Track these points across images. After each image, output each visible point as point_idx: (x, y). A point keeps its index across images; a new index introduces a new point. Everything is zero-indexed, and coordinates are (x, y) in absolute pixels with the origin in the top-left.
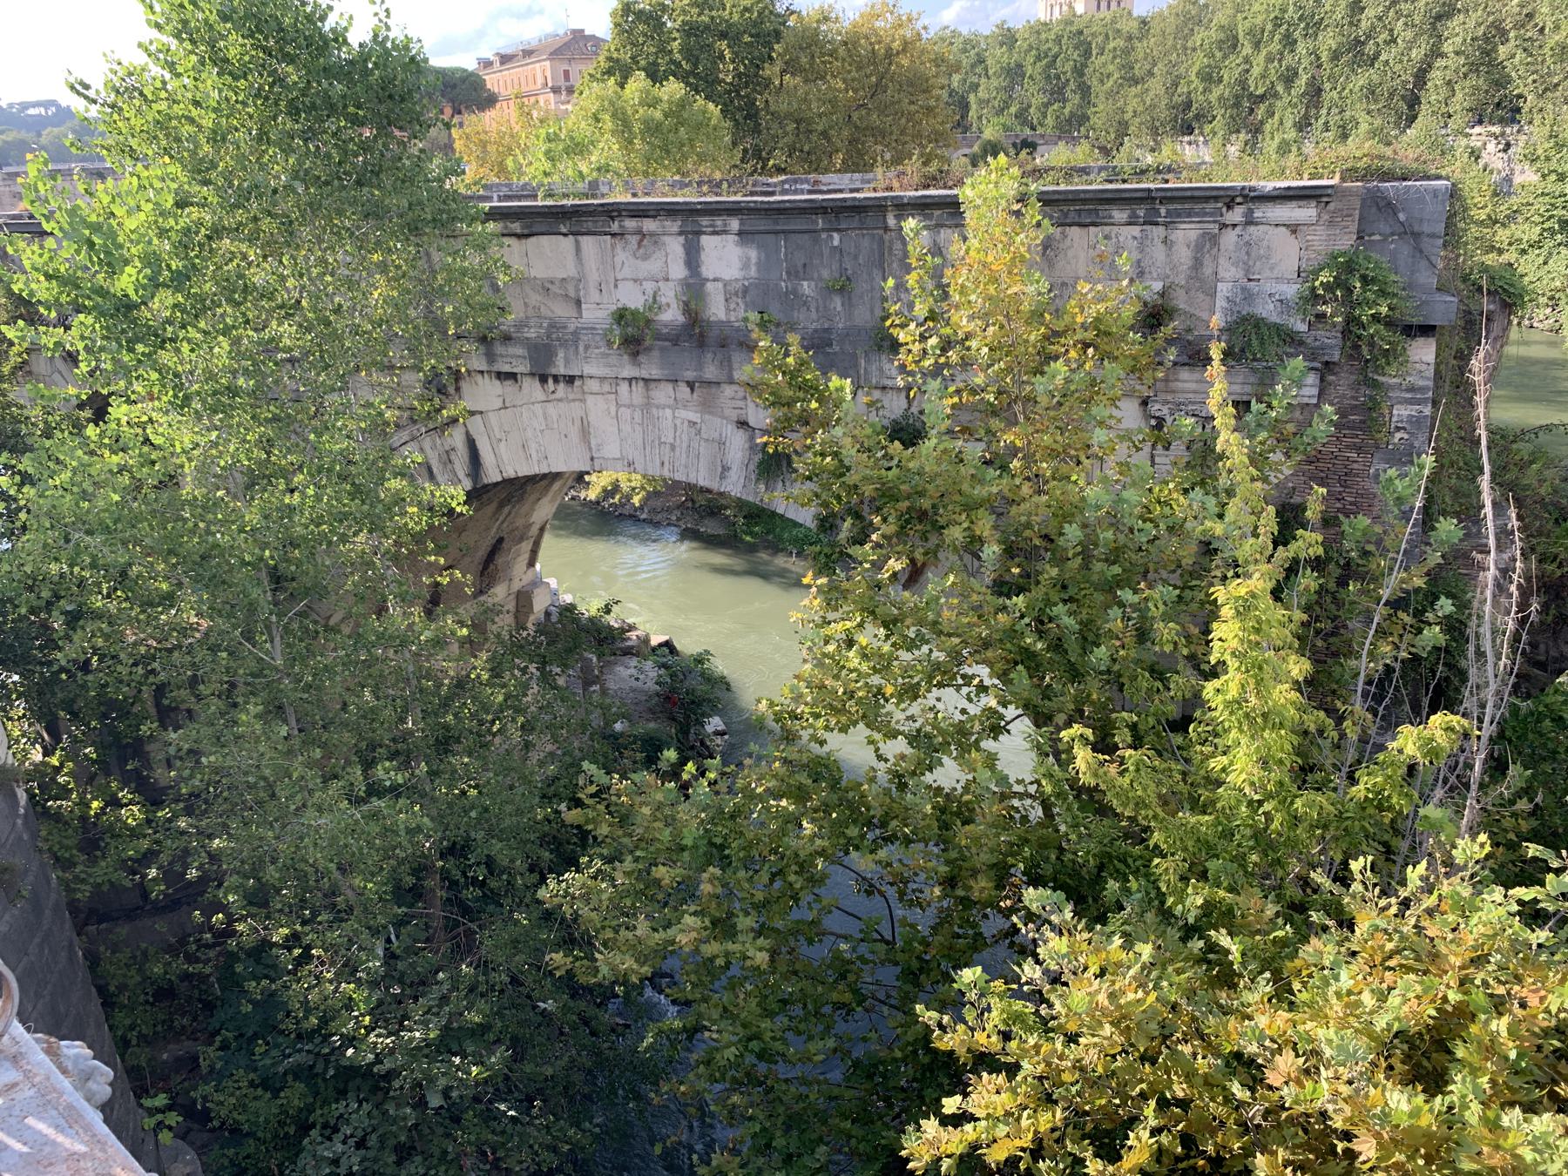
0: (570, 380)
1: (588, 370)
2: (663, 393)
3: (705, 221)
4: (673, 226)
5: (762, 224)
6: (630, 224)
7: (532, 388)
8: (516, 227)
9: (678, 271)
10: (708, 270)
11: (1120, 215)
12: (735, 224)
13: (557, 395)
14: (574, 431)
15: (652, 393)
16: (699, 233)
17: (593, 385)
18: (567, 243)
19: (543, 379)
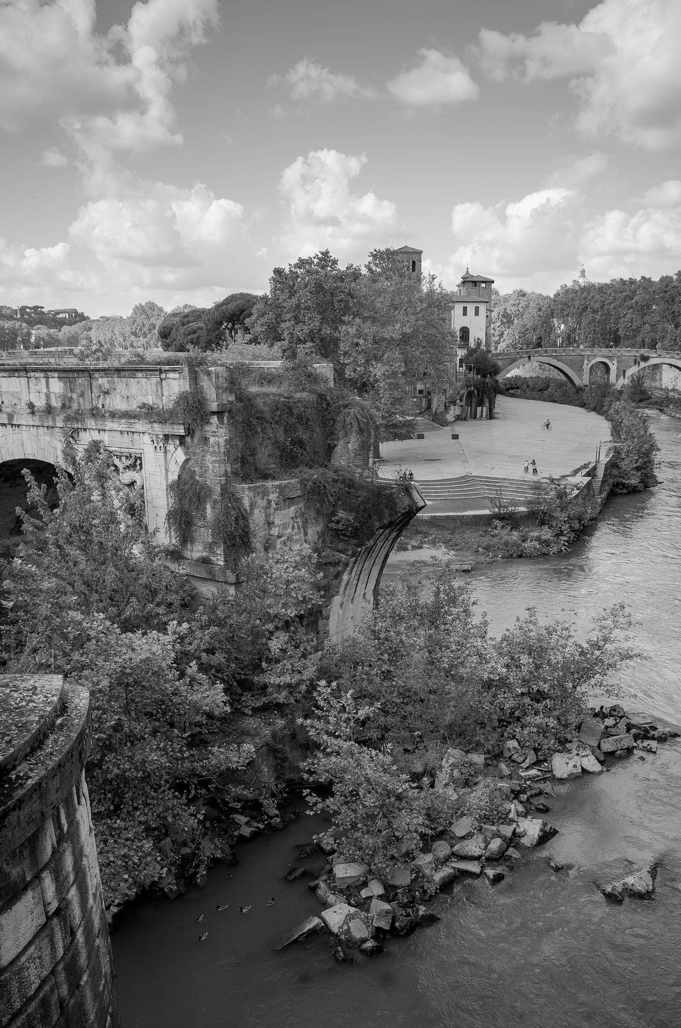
0: (19, 426)
1: (22, 422)
2: (41, 430)
3: (49, 374)
4: (42, 375)
5: (63, 375)
6: (32, 374)
7: (9, 427)
8: (5, 374)
9: (44, 390)
10: (51, 390)
11: (139, 375)
12: (56, 375)
13: (16, 431)
14: (20, 444)
15: (39, 431)
16: (49, 378)
17: (24, 428)
18: (18, 379)
19: (12, 425)
